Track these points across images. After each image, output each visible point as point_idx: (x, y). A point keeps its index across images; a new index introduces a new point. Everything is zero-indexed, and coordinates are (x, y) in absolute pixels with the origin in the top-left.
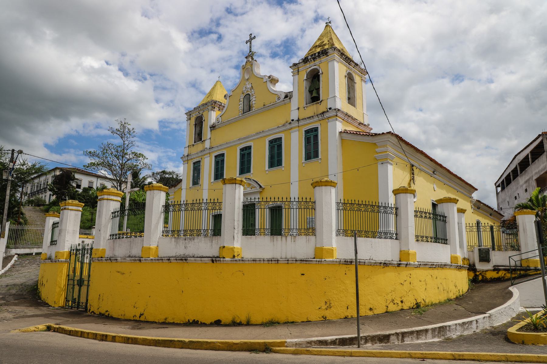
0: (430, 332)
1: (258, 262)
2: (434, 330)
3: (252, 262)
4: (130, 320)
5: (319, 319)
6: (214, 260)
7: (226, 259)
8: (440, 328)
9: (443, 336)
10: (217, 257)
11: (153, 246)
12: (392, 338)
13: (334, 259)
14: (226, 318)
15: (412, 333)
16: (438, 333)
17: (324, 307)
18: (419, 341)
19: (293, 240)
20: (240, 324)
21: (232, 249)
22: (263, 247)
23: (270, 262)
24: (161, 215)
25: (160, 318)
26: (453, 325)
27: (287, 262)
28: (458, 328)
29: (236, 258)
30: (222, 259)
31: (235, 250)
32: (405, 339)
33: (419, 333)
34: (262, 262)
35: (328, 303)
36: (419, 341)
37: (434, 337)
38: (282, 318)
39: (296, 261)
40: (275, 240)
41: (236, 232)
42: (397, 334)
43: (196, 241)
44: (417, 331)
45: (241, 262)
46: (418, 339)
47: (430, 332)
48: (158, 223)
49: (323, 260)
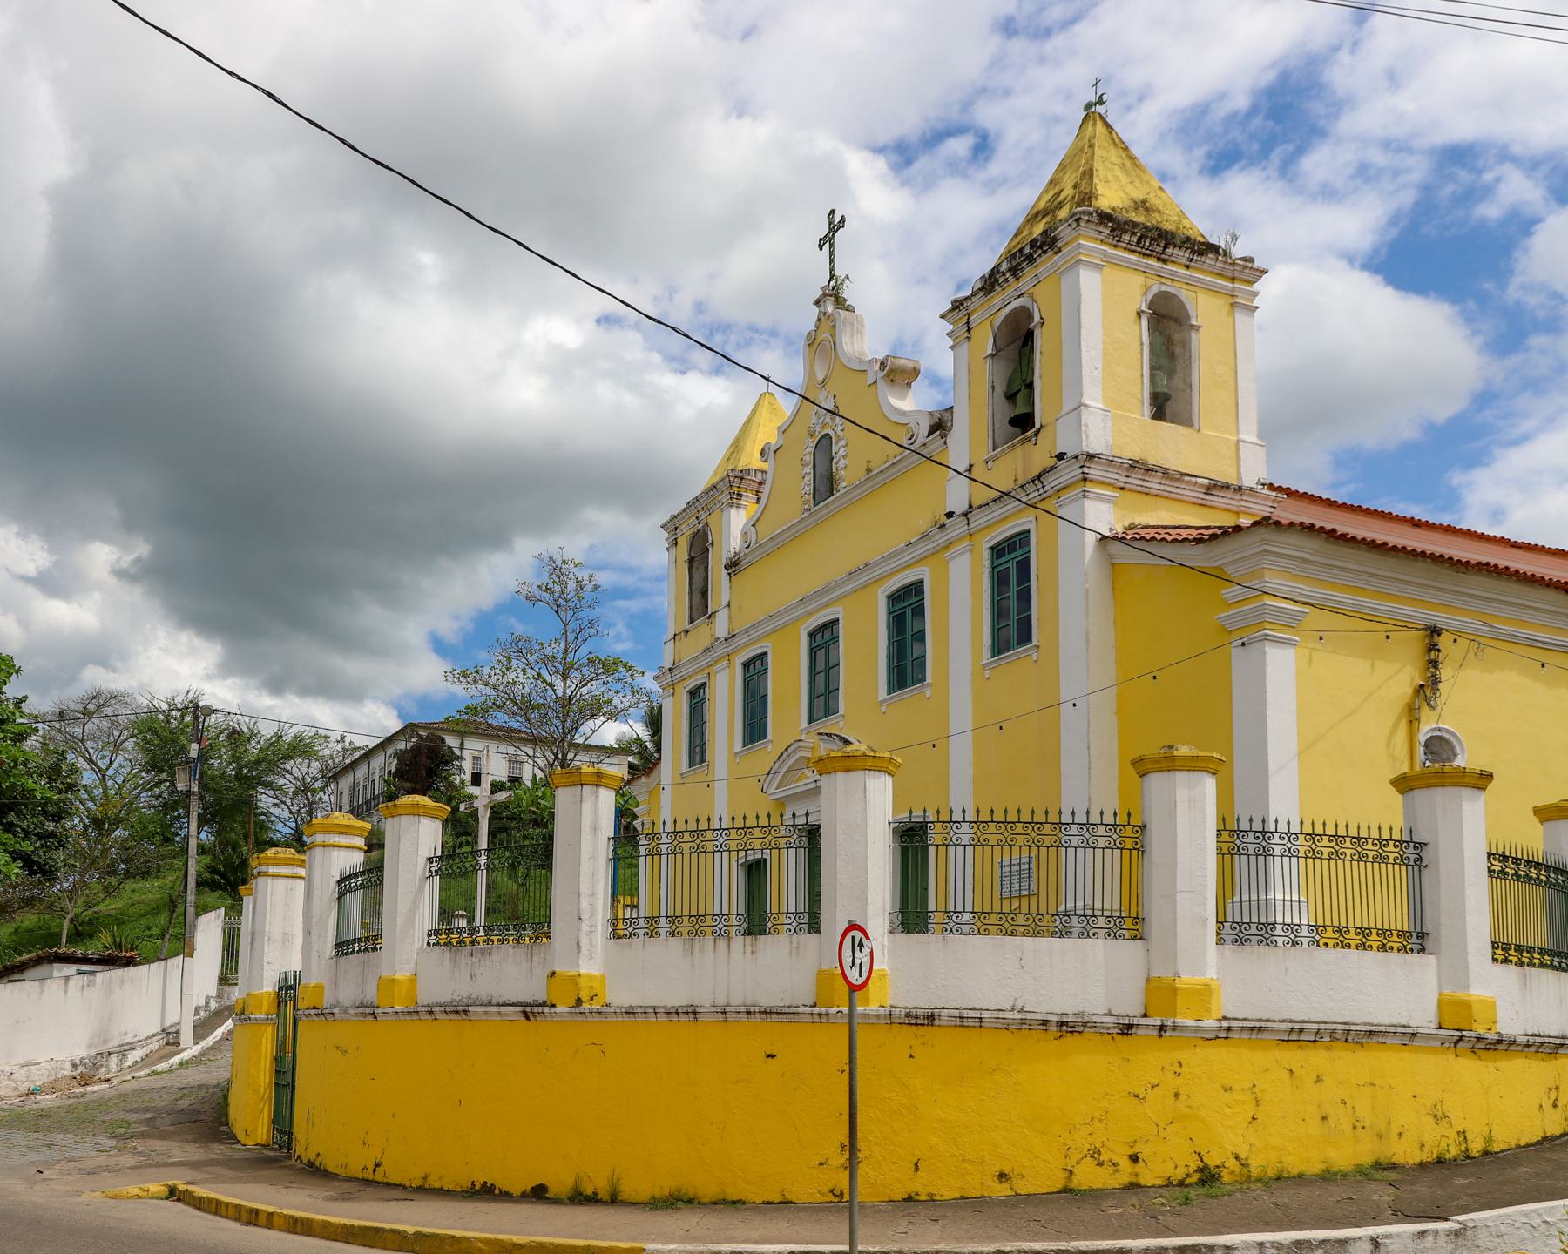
1: (641, 1018)
3: (626, 1017)
4: (357, 1179)
6: (530, 1011)
7: (559, 1009)
10: (544, 1004)
11: (403, 974)
14: (559, 1184)
19: (748, 948)
20: (592, 1200)
21: (574, 980)
22: (664, 974)
23: (675, 1018)
24: (422, 885)
25: (412, 1176)
27: (721, 1017)
29: (586, 1006)
30: (547, 1009)
31: (583, 983)
34: (652, 1018)
38: (708, 1188)
39: (748, 1013)
40: (696, 950)
41: (585, 927)
43: (495, 957)
45: (597, 1018)
48: (413, 910)
49: (833, 1011)
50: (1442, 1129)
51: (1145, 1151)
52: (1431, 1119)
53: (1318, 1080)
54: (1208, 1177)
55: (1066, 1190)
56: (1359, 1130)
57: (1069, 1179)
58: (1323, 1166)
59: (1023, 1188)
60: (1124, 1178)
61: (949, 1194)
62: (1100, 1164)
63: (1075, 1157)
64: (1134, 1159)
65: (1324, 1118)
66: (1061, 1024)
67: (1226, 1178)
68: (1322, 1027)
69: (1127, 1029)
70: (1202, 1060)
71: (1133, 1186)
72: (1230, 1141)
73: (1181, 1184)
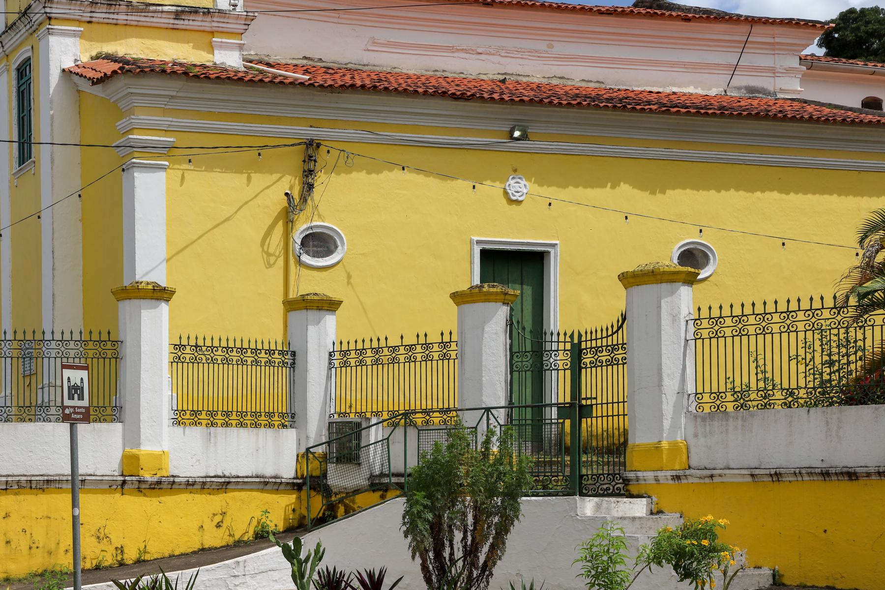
50: (104, 545)
52: (94, 539)
56: (34, 550)
58: (4, 575)
65: (8, 542)
68: (10, 479)
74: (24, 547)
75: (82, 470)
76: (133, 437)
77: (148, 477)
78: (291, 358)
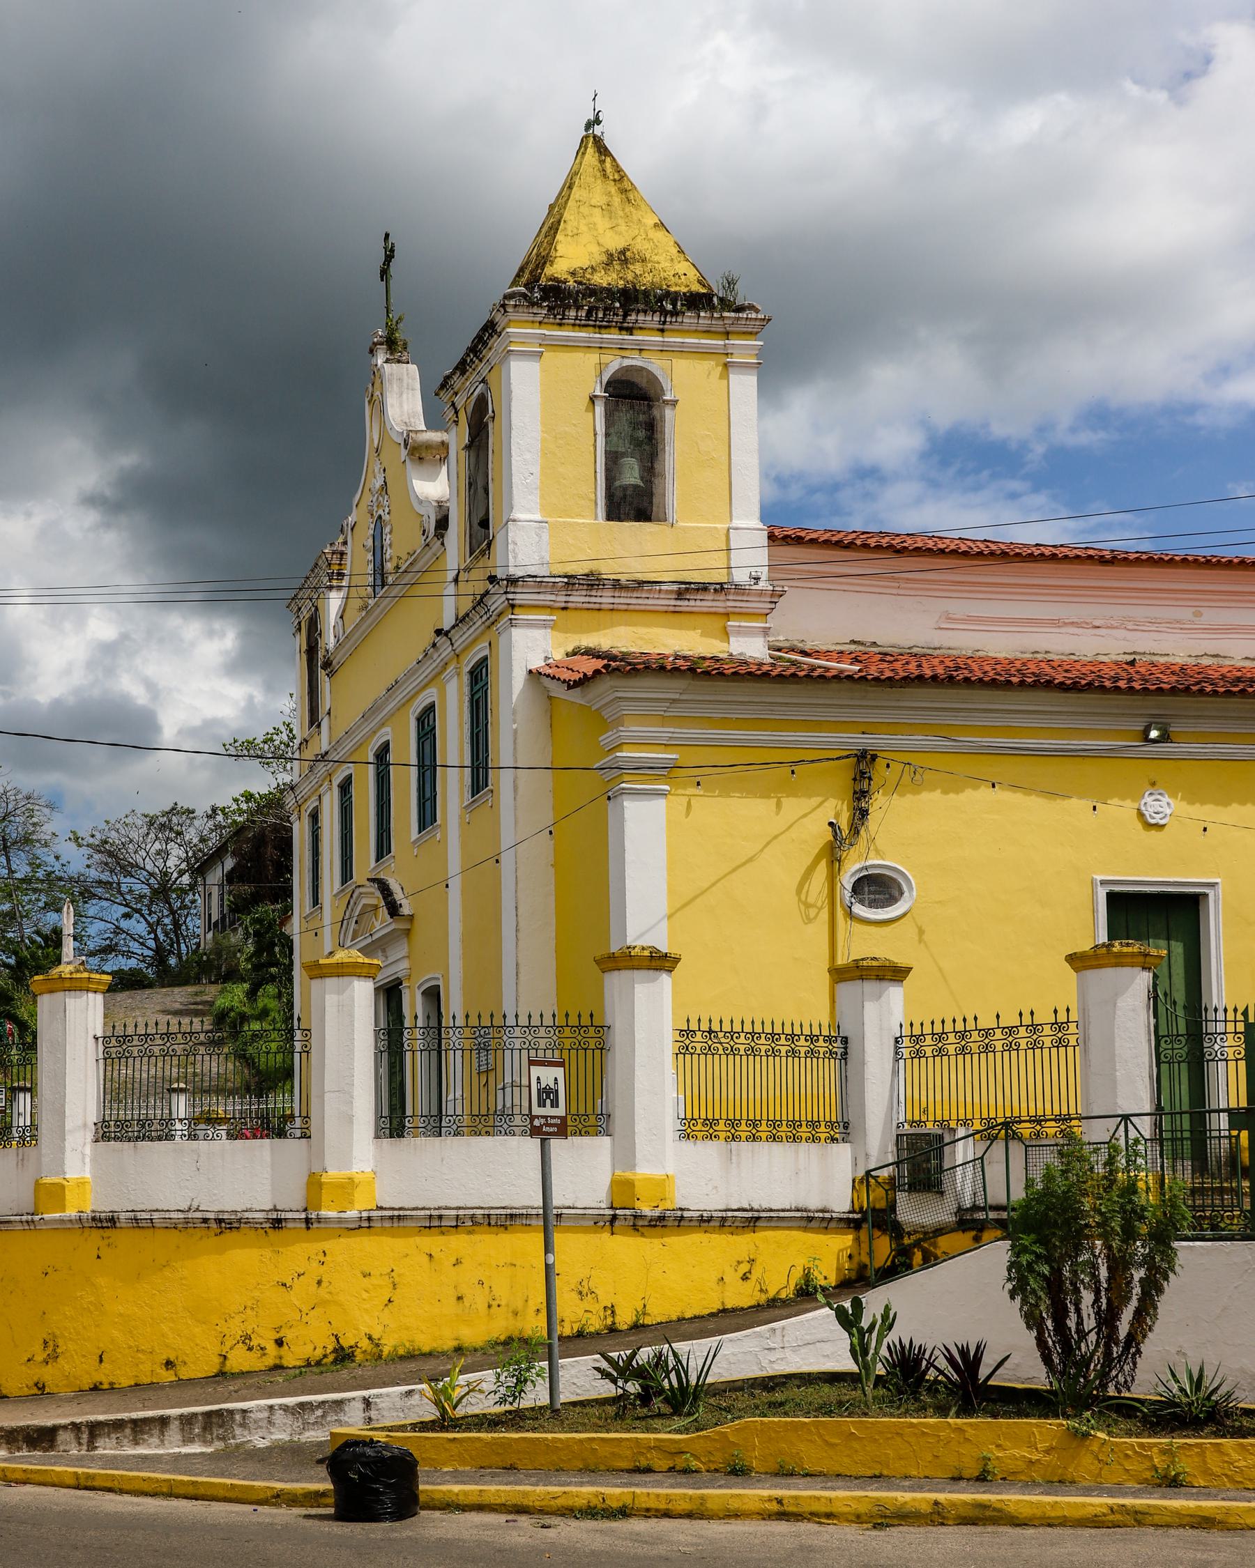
0: (175, 1425)
2: (187, 1421)
5: (26, 1391)
8: (208, 1414)
9: (223, 1439)
12: (62, 1436)
13: (71, 1213)
15: (118, 1425)
16: (204, 1429)
17: (39, 1358)
18: (141, 1450)
26: (260, 1409)
28: (279, 1416)
32: (99, 1443)
33: (139, 1428)
35: (51, 1343)
36: (141, 1450)
37: (187, 1440)
42: (76, 1427)
44: (134, 1422)
46: (136, 1443)
47: (175, 1425)
50: (588, 1303)
51: (289, 1335)
52: (575, 1296)
53: (458, 1262)
54: (343, 1356)
55: (221, 1374)
56: (494, 1308)
57: (223, 1364)
58: (455, 1343)
59: (185, 1373)
60: (270, 1361)
61: (125, 1382)
62: (250, 1349)
63: (229, 1344)
64: (279, 1343)
65: (459, 1298)
66: (219, 1221)
67: (359, 1357)
68: (461, 1212)
69: (277, 1224)
70: (340, 1247)
71: (278, 1367)
72: (366, 1321)
73: (318, 1363)
74: (482, 1307)
75: (557, 1200)
76: (625, 1155)
77: (647, 1210)
78: (842, 1047)
